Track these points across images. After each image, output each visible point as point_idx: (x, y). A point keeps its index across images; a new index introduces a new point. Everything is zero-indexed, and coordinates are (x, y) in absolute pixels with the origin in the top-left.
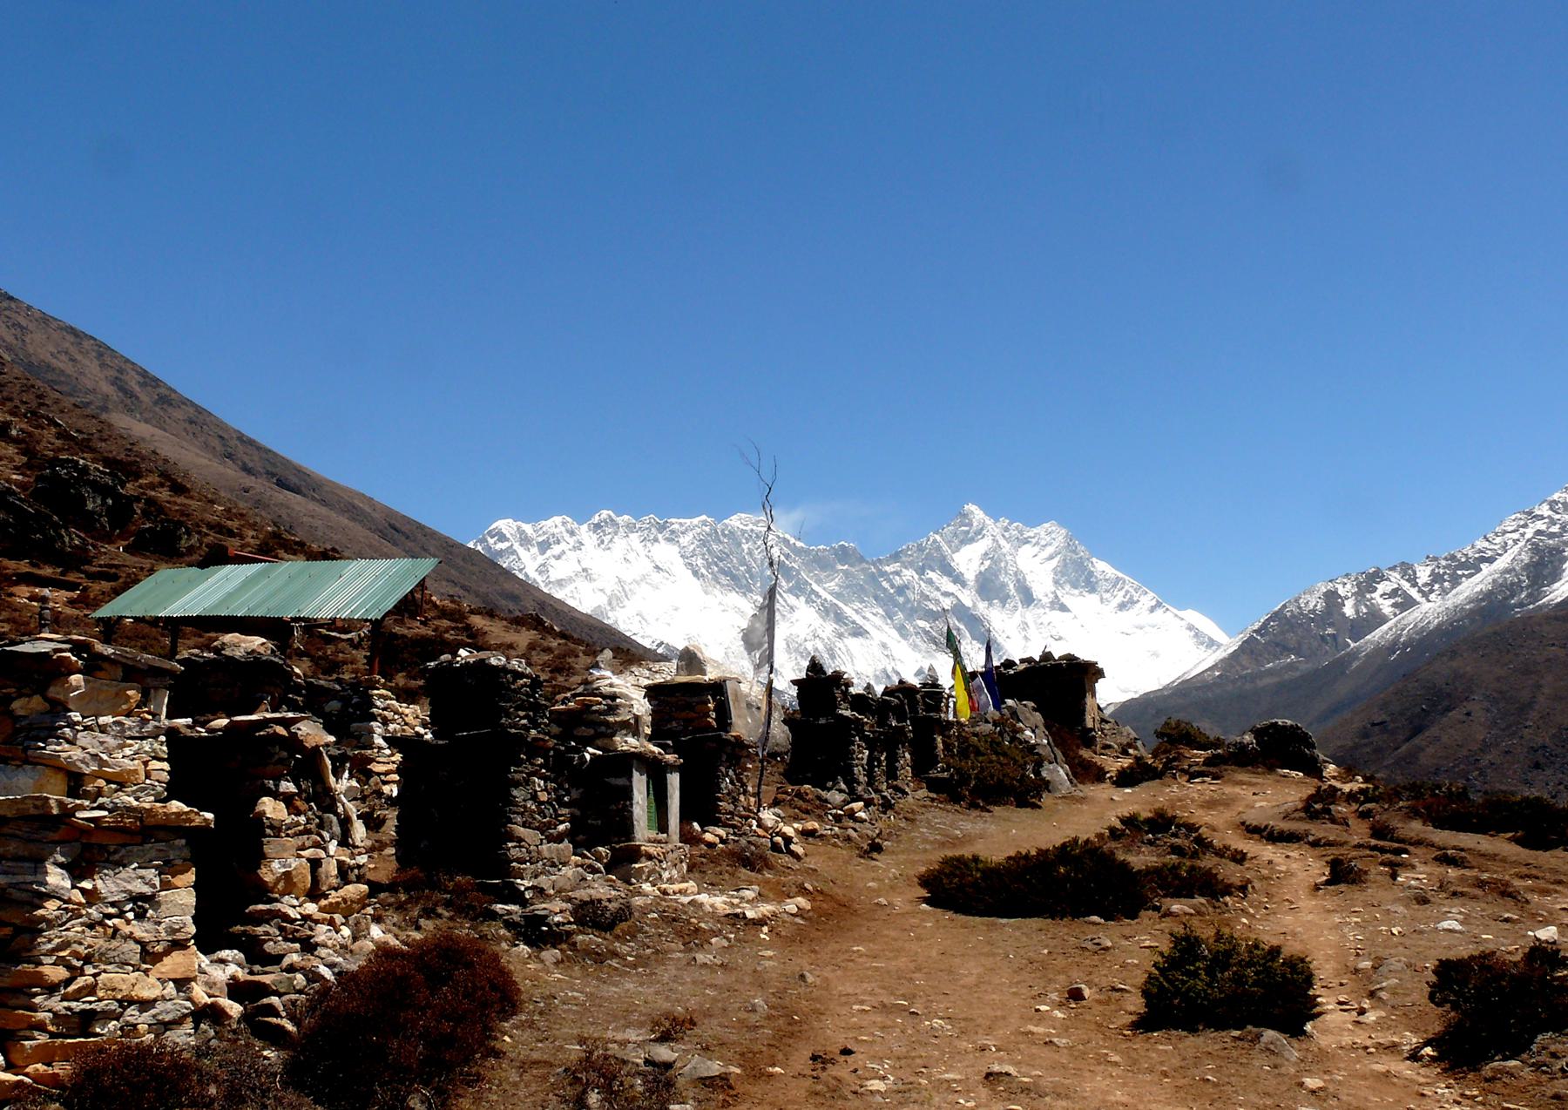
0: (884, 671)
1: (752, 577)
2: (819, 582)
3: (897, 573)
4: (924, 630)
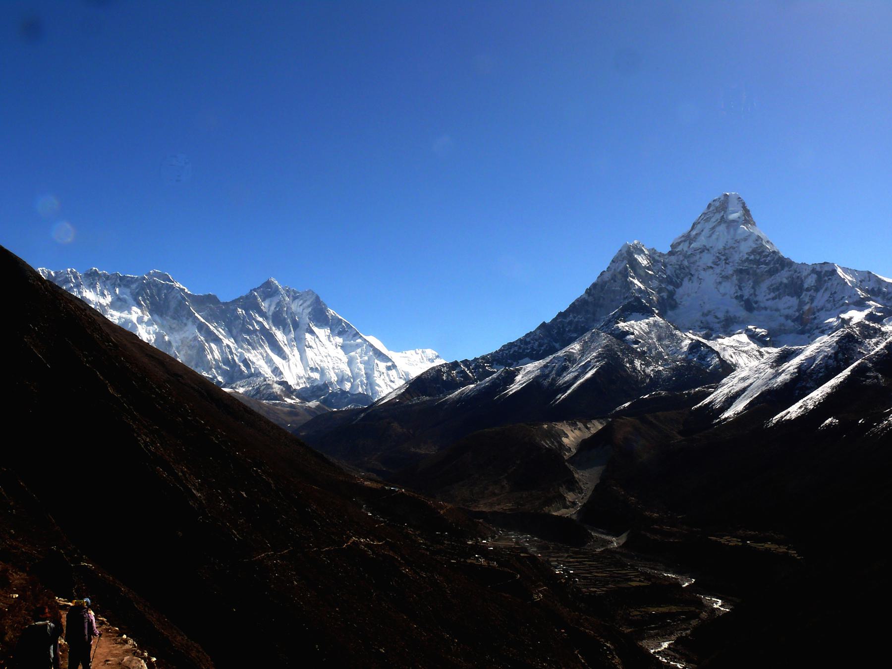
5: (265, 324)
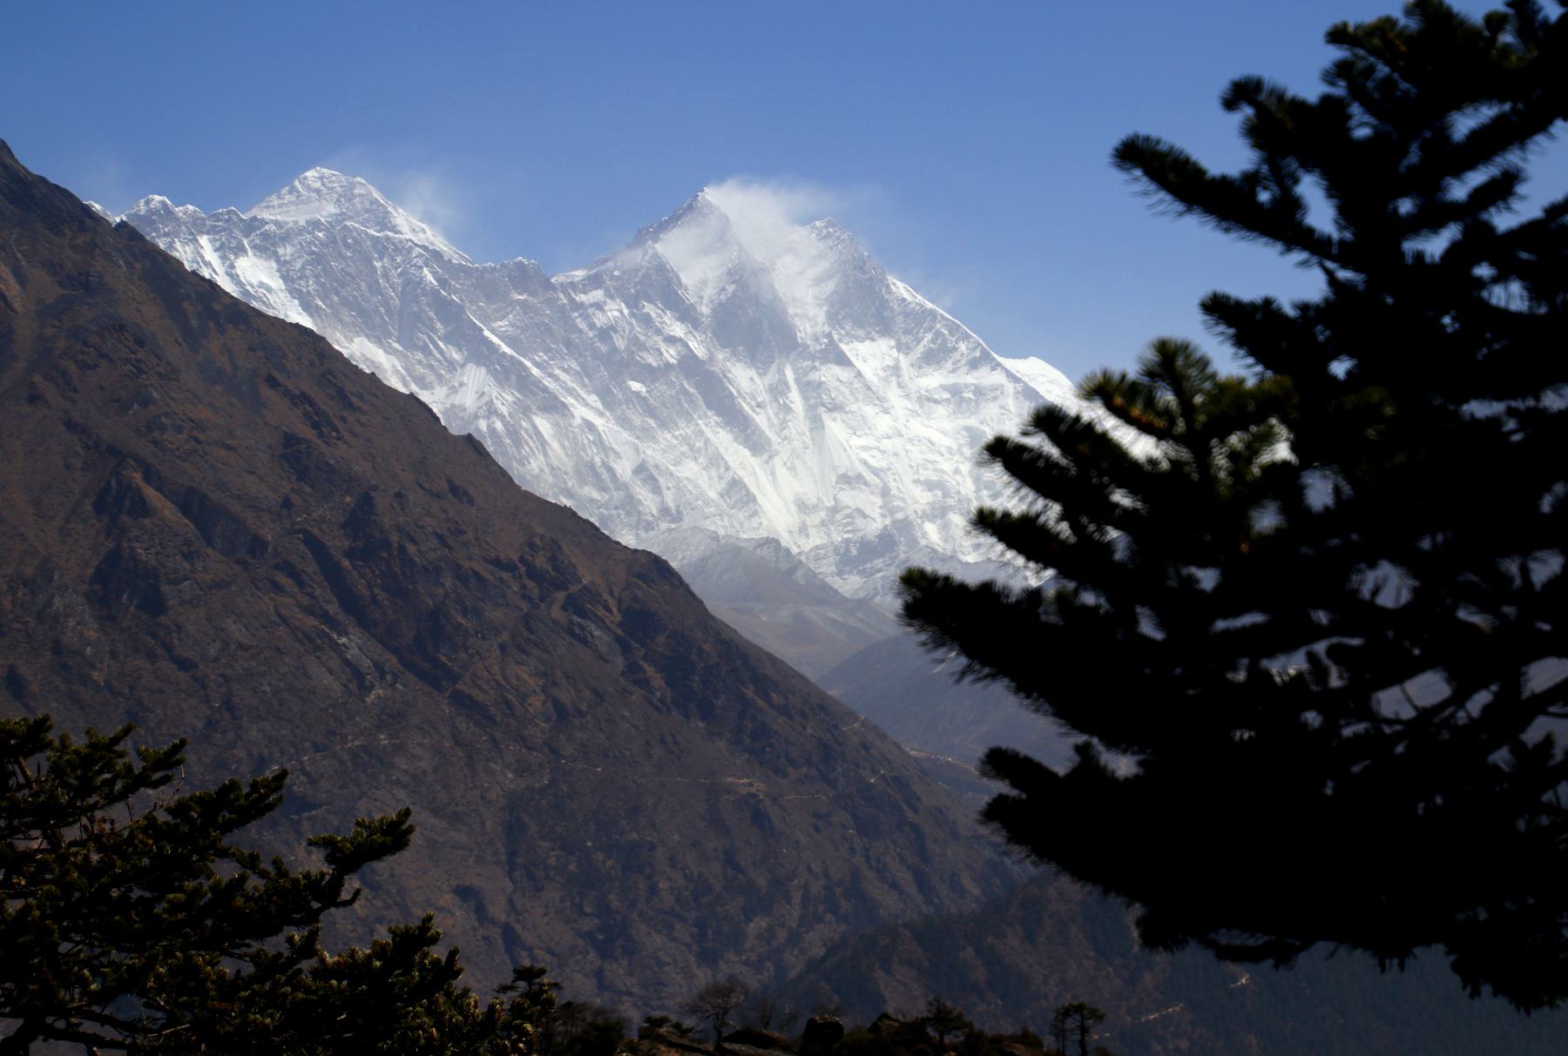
0: (592, 466)
1: (389, 311)
2: (486, 319)
3: (599, 306)
4: (638, 394)
5: (693, 344)
